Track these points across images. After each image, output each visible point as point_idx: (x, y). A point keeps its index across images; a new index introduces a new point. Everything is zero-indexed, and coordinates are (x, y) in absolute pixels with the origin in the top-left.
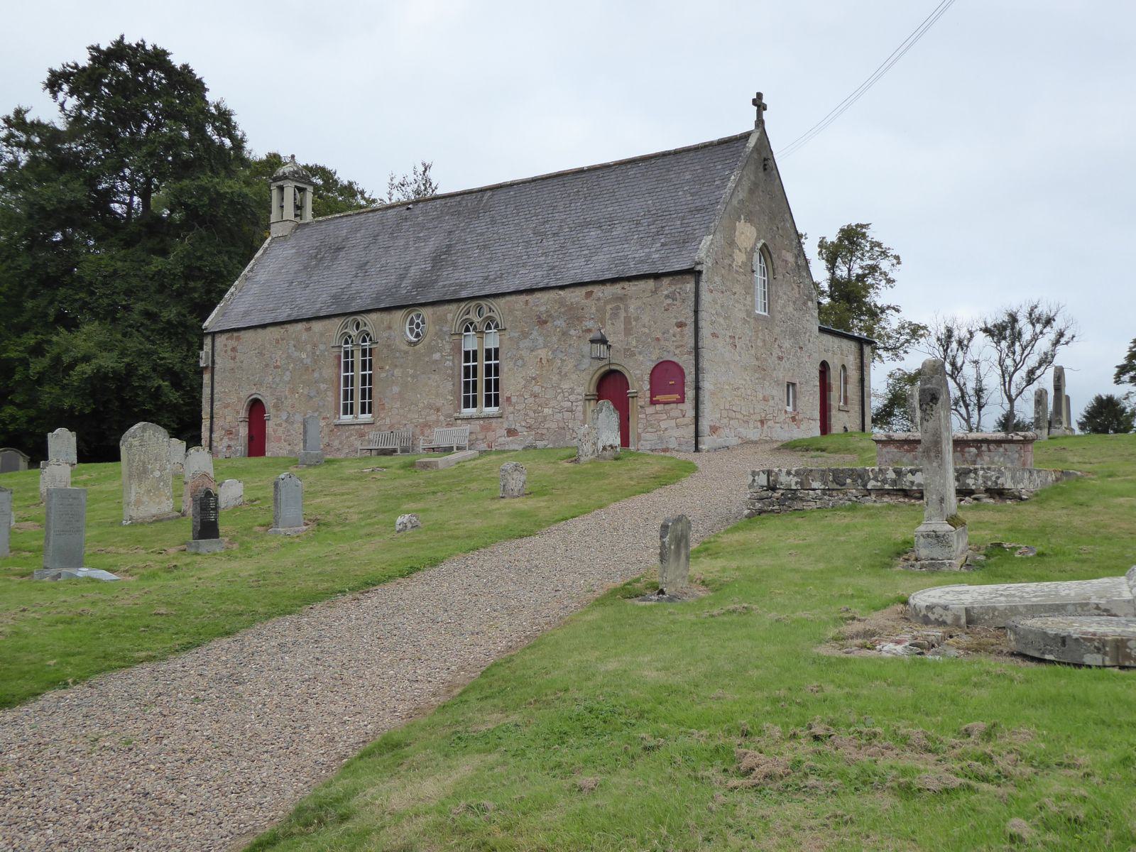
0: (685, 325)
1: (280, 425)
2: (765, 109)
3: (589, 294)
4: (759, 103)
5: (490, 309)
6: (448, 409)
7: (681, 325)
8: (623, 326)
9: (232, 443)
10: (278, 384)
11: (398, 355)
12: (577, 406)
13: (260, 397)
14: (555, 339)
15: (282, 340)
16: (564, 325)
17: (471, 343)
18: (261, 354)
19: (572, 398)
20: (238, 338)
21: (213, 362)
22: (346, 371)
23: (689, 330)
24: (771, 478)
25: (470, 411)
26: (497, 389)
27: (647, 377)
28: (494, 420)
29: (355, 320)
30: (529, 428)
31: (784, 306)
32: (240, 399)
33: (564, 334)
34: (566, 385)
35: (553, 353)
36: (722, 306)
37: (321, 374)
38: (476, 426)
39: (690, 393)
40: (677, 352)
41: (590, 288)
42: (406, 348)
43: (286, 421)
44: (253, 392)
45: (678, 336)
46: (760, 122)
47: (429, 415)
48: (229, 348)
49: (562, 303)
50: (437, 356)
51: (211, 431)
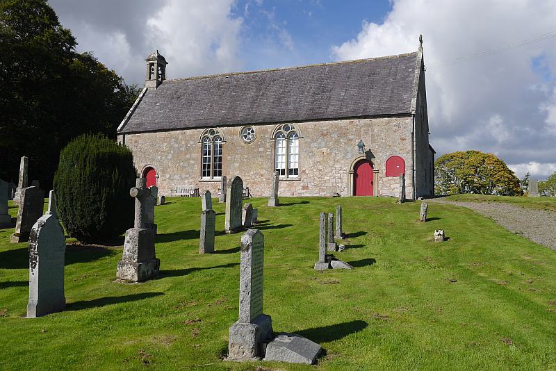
0: (405, 139)
4: (421, 41)
11: (238, 148)
19: (341, 172)
33: (337, 142)
34: (338, 166)
46: (421, 48)
49: (336, 126)
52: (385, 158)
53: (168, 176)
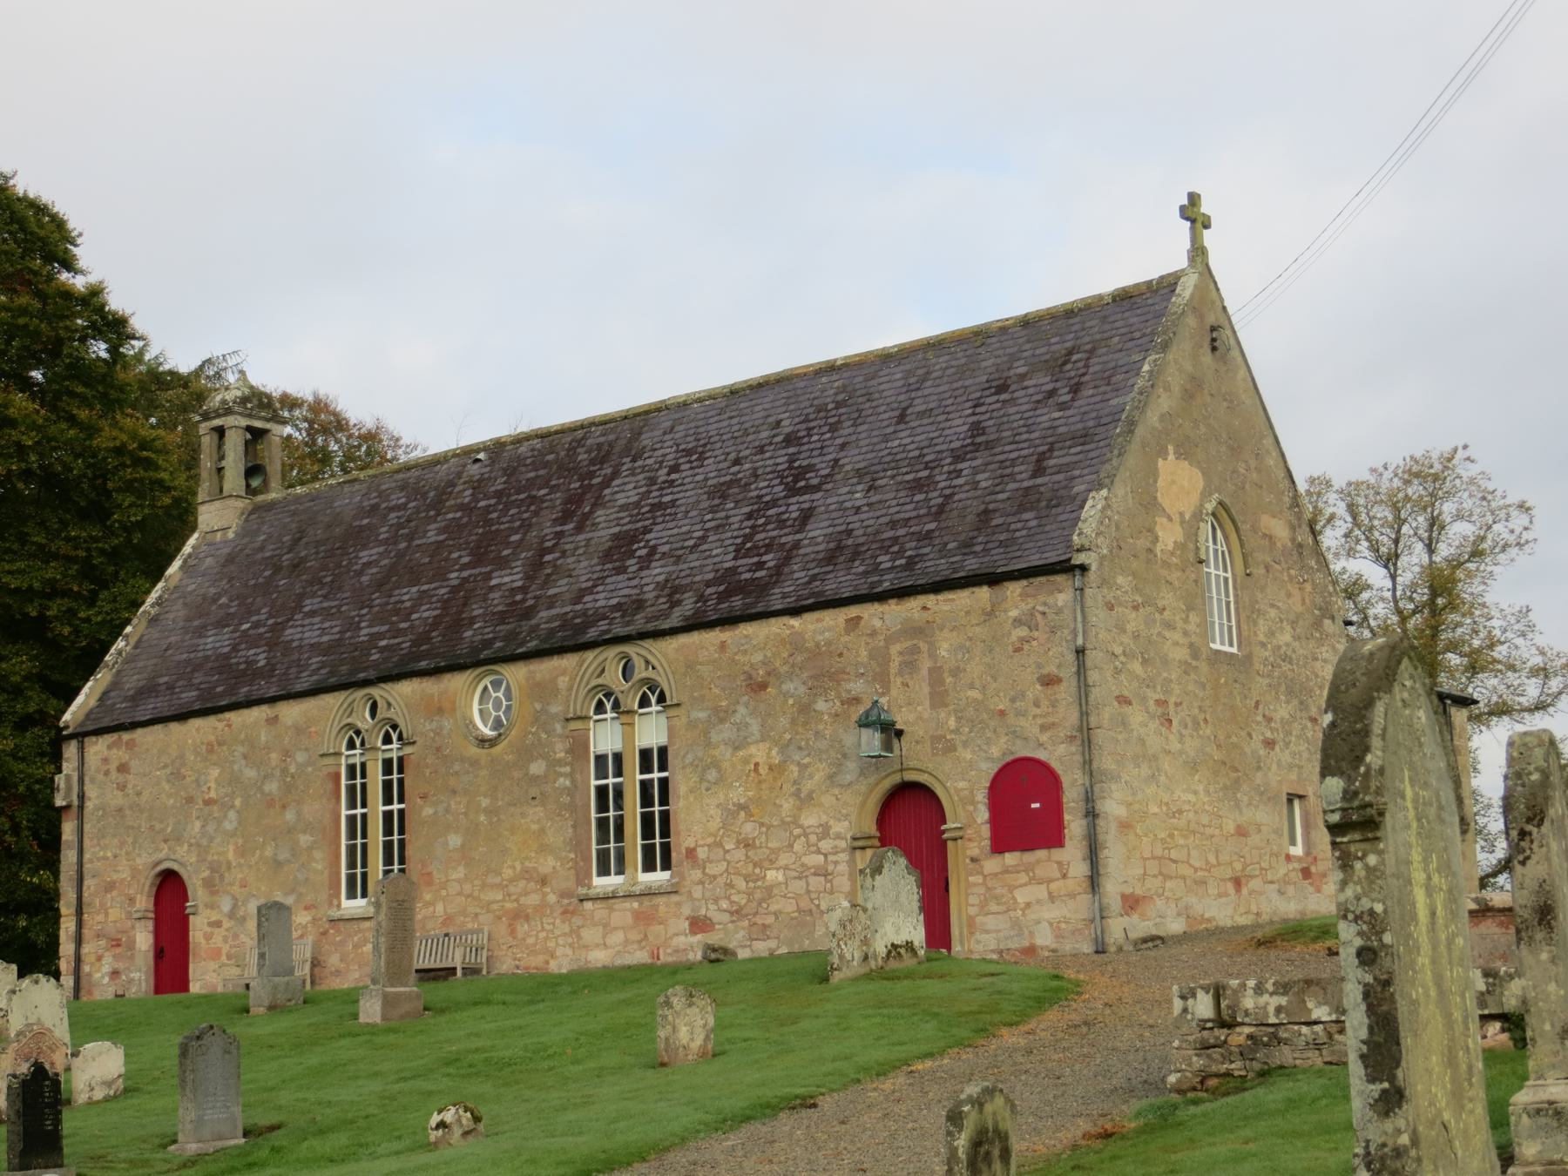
0: (1059, 680)
1: (218, 924)
2: (1207, 226)
3: (854, 622)
4: (1193, 213)
5: (647, 662)
6: (565, 880)
7: (1049, 681)
8: (926, 690)
9: (121, 966)
10: (211, 839)
11: (457, 767)
12: (836, 863)
13: (176, 867)
14: (784, 721)
15: (220, 744)
16: (802, 689)
17: (606, 737)
18: (177, 776)
19: (825, 845)
20: (131, 745)
21: (82, 797)
22: (352, 805)
23: (1066, 692)
24: (1224, 1004)
25: (613, 881)
26: (665, 833)
27: (981, 796)
28: (661, 900)
29: (370, 697)
30: (737, 913)
31: (1271, 634)
32: (135, 873)
33: (805, 709)
34: (810, 820)
35: (782, 751)
36: (1136, 637)
37: (298, 814)
38: (623, 913)
39: (1074, 825)
40: (1044, 738)
41: (853, 611)
42: (474, 751)
43: (232, 915)
44: (162, 855)
45: (1045, 703)
46: (1198, 252)
47: (526, 894)
48: (113, 766)
49: (795, 643)
50: (537, 768)
51: (79, 940)
52: (987, 770)
53: (226, 905)
